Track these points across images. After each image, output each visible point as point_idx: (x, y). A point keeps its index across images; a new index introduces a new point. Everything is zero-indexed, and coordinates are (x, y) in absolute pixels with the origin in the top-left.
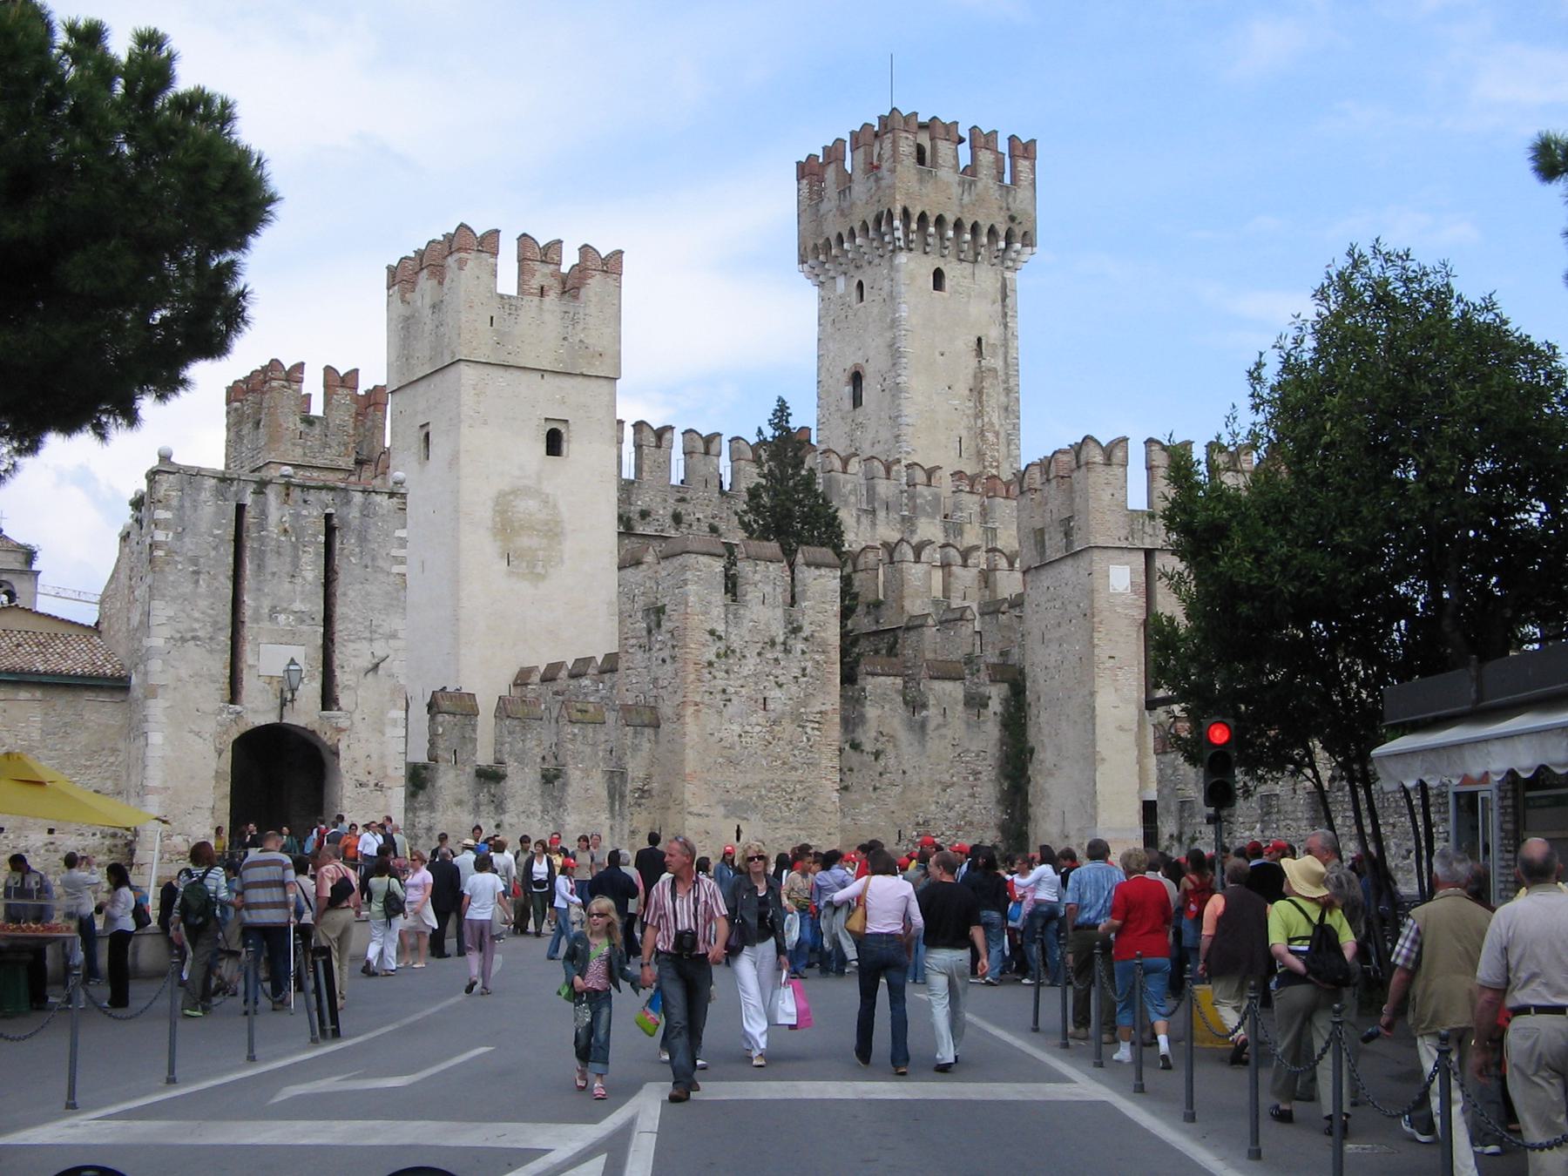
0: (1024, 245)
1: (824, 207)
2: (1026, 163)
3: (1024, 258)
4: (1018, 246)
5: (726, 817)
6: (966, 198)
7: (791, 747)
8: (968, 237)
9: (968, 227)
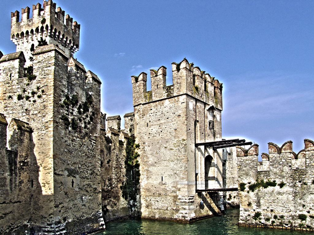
0: (76, 48)
1: (22, 24)
2: (78, 29)
3: (76, 51)
4: (75, 47)
5: (68, 176)
6: (65, 30)
7: (88, 148)
8: (65, 39)
9: (65, 37)
